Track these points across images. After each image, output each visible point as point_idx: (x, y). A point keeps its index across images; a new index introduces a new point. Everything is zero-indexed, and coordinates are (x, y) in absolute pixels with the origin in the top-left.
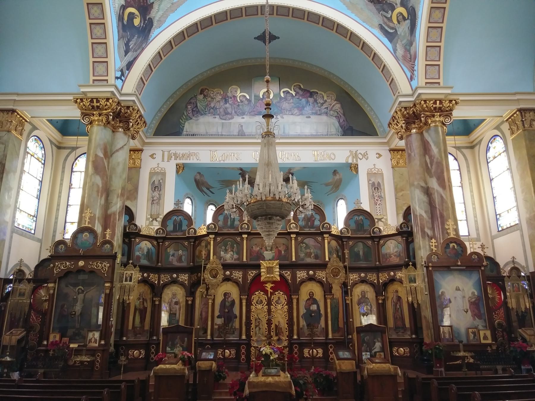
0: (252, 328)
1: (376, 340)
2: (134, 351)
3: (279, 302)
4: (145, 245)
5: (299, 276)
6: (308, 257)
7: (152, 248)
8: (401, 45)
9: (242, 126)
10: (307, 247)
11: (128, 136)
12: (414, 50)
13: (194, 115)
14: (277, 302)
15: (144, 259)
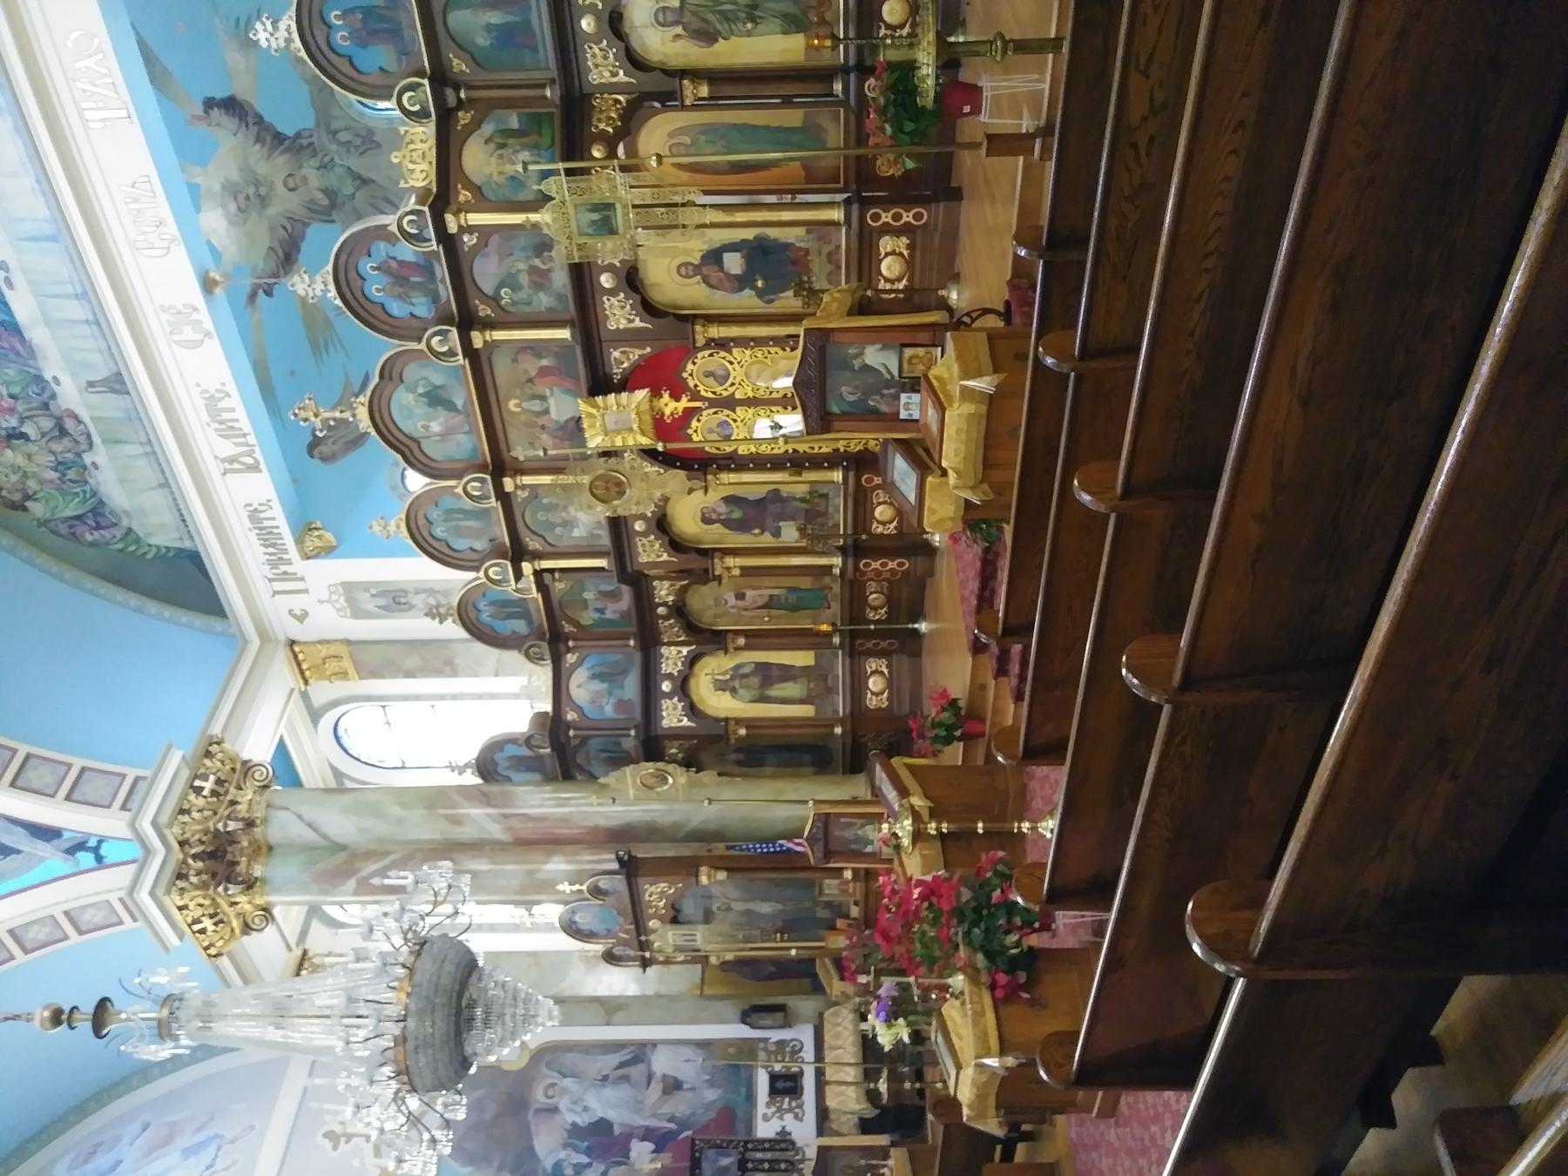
0: (809, 451)
1: (857, 364)
2: (873, 693)
3: (721, 373)
4: (582, 688)
5: (623, 321)
6: (550, 280)
7: (587, 664)
9: (91, 384)
10: (510, 281)
11: (272, 812)
13: (115, 525)
14: (723, 378)
15: (622, 688)
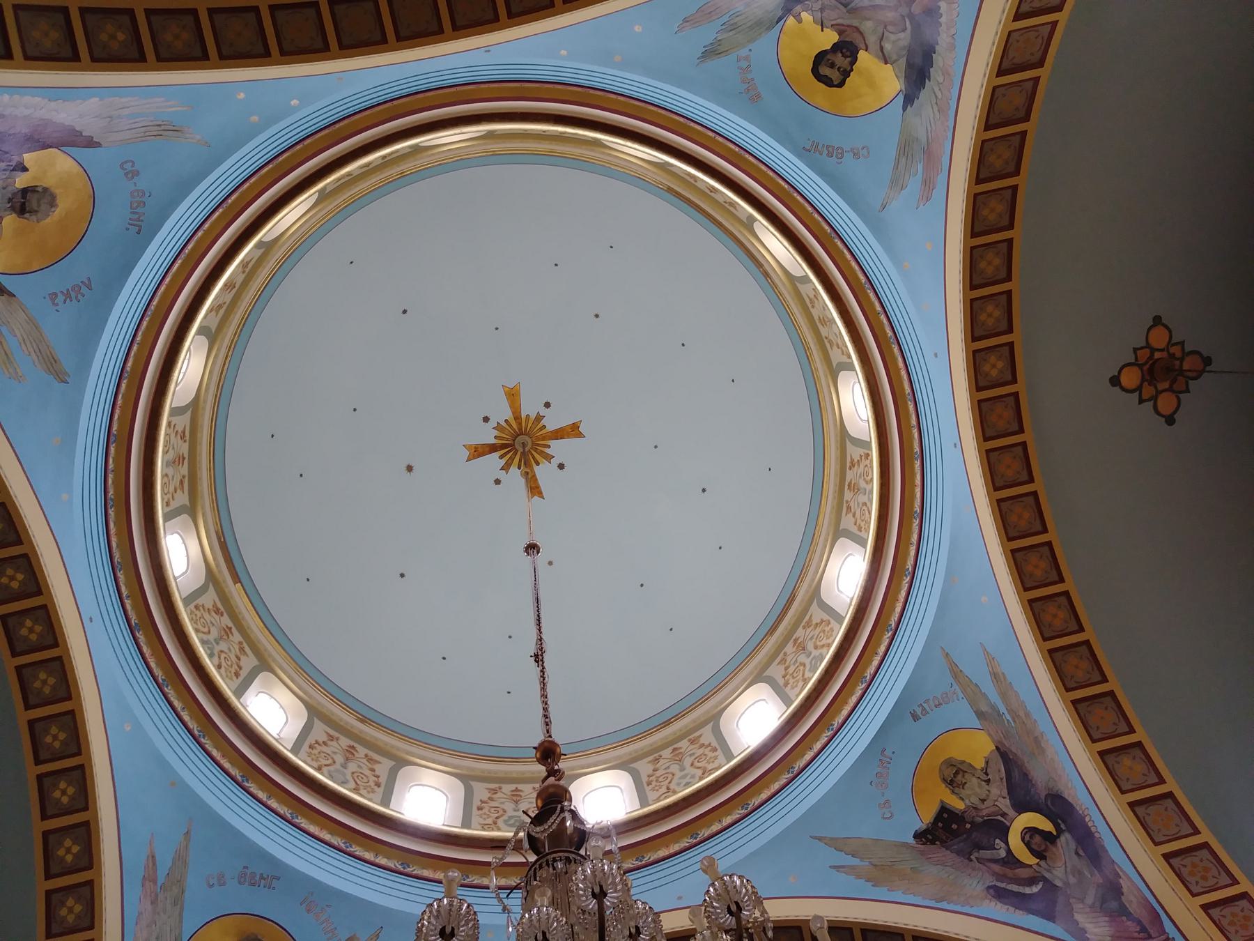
8: (1088, 910)
12: (1134, 900)
